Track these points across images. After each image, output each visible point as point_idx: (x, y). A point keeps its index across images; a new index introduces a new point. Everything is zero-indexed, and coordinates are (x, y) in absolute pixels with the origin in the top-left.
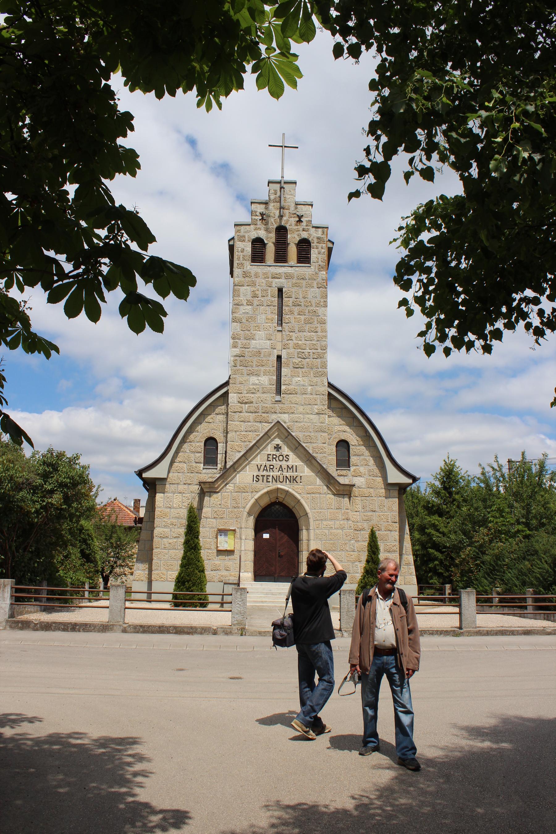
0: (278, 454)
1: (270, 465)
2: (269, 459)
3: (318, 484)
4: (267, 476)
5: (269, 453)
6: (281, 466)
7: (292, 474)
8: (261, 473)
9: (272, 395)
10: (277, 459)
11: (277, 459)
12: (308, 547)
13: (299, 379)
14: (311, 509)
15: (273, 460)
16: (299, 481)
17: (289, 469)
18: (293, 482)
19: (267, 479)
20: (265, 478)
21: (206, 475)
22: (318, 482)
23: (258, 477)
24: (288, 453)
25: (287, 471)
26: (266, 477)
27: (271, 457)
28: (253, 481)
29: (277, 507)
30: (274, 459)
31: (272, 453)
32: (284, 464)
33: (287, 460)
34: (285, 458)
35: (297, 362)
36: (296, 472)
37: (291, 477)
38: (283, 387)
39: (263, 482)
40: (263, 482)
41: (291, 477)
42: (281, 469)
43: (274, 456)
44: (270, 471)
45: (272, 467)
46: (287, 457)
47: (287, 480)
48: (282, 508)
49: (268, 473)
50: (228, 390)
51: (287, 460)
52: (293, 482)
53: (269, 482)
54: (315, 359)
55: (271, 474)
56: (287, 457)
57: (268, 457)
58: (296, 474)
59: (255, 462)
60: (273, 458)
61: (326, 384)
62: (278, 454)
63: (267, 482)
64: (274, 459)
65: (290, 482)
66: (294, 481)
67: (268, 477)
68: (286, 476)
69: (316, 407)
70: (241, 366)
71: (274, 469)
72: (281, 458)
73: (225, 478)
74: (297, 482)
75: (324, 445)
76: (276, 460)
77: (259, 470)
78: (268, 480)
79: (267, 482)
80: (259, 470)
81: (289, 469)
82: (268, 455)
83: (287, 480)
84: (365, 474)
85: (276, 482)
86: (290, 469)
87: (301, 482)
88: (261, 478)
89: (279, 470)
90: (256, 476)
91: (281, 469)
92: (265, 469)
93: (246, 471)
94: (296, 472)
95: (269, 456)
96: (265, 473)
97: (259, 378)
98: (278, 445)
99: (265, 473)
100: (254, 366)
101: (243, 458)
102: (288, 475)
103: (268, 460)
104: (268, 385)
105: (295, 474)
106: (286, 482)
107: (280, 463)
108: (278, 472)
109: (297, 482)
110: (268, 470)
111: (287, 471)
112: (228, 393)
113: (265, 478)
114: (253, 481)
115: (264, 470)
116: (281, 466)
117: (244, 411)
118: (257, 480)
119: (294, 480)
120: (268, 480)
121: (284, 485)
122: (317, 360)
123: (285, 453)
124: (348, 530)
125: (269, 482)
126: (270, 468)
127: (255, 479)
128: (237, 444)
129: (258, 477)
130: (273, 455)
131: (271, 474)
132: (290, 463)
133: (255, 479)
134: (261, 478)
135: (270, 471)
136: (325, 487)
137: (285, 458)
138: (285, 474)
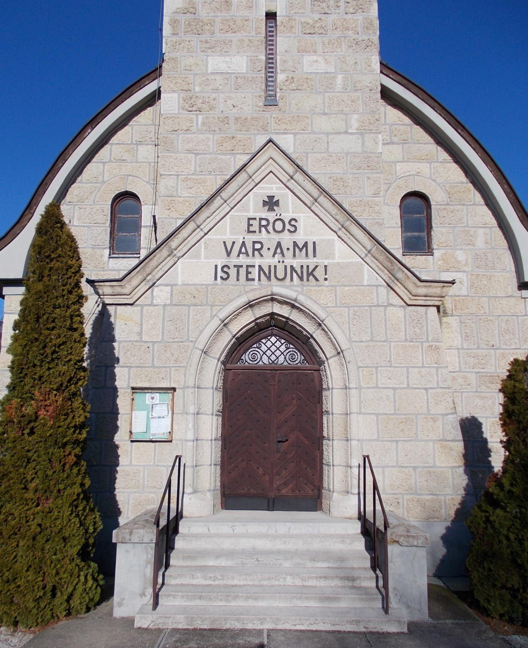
0: (271, 216)
1: (254, 243)
2: (251, 229)
3: (365, 284)
4: (248, 266)
5: (251, 215)
6: (279, 245)
7: (305, 262)
8: (234, 260)
9: (258, 94)
10: (270, 228)
11: (270, 228)
12: (346, 430)
13: (315, 58)
14: (350, 340)
15: (260, 231)
16: (321, 277)
17: (297, 250)
18: (308, 280)
19: (248, 273)
20: (243, 271)
21: (114, 272)
22: (366, 277)
23: (226, 269)
24: (294, 216)
25: (294, 255)
26: (244, 268)
27: (256, 223)
28: (216, 279)
29: (273, 339)
30: (263, 229)
31: (258, 215)
32: (287, 239)
33: (292, 229)
34: (288, 227)
35: (311, 22)
36: (314, 256)
37: (302, 266)
38: (281, 77)
39: (238, 280)
40: (238, 280)
41: (302, 266)
42: (279, 251)
43: (264, 223)
44: (253, 255)
45: (258, 246)
46: (293, 223)
47: (294, 274)
48: (283, 341)
49: (249, 261)
50: (159, 88)
51: (292, 229)
52: (308, 280)
53: (253, 280)
54: (350, 16)
55: (257, 261)
56: (293, 223)
57: (249, 225)
58: (315, 260)
59: (219, 237)
60: (261, 226)
61: (377, 67)
62: (271, 216)
63: (248, 279)
64: (263, 229)
65: (301, 278)
66: (311, 277)
67: (250, 269)
68: (292, 266)
69: (355, 116)
70: (186, 32)
71: (264, 251)
72: (279, 226)
73: (148, 270)
74: (317, 280)
75: (377, 199)
76: (268, 232)
77: (229, 254)
78: (250, 276)
79: (248, 279)
80: (229, 254)
81: (297, 250)
82: (249, 219)
83: (294, 274)
84: (465, 265)
85: (269, 278)
86: (301, 250)
87: (326, 279)
88: (233, 272)
89: (275, 253)
90: (223, 268)
91: (279, 251)
92: (243, 250)
93: (197, 256)
94: (315, 256)
95: (251, 222)
96: (243, 260)
97: (228, 59)
98: (271, 198)
99: (243, 260)
100: (217, 31)
101: (191, 226)
102: (296, 263)
103: (249, 232)
104: (247, 73)
105: (311, 262)
106: (292, 279)
107: (276, 238)
108: (274, 256)
109: (317, 280)
110: (250, 252)
111: (294, 255)
112: (160, 92)
113: (243, 271)
114: (216, 279)
115: (240, 252)
116: (279, 245)
117: (194, 129)
118: (225, 276)
119: (311, 274)
120: (250, 276)
121: (287, 287)
122: (354, 17)
123: (286, 217)
124: (440, 390)
125: (253, 280)
126: (254, 250)
127: (220, 274)
128: (181, 199)
129: (226, 269)
130: (261, 219)
131: (257, 261)
132: (300, 237)
133: (220, 274)
134: (233, 272)
135: (253, 255)
136: (384, 291)
137: (288, 227)
138: (289, 261)
